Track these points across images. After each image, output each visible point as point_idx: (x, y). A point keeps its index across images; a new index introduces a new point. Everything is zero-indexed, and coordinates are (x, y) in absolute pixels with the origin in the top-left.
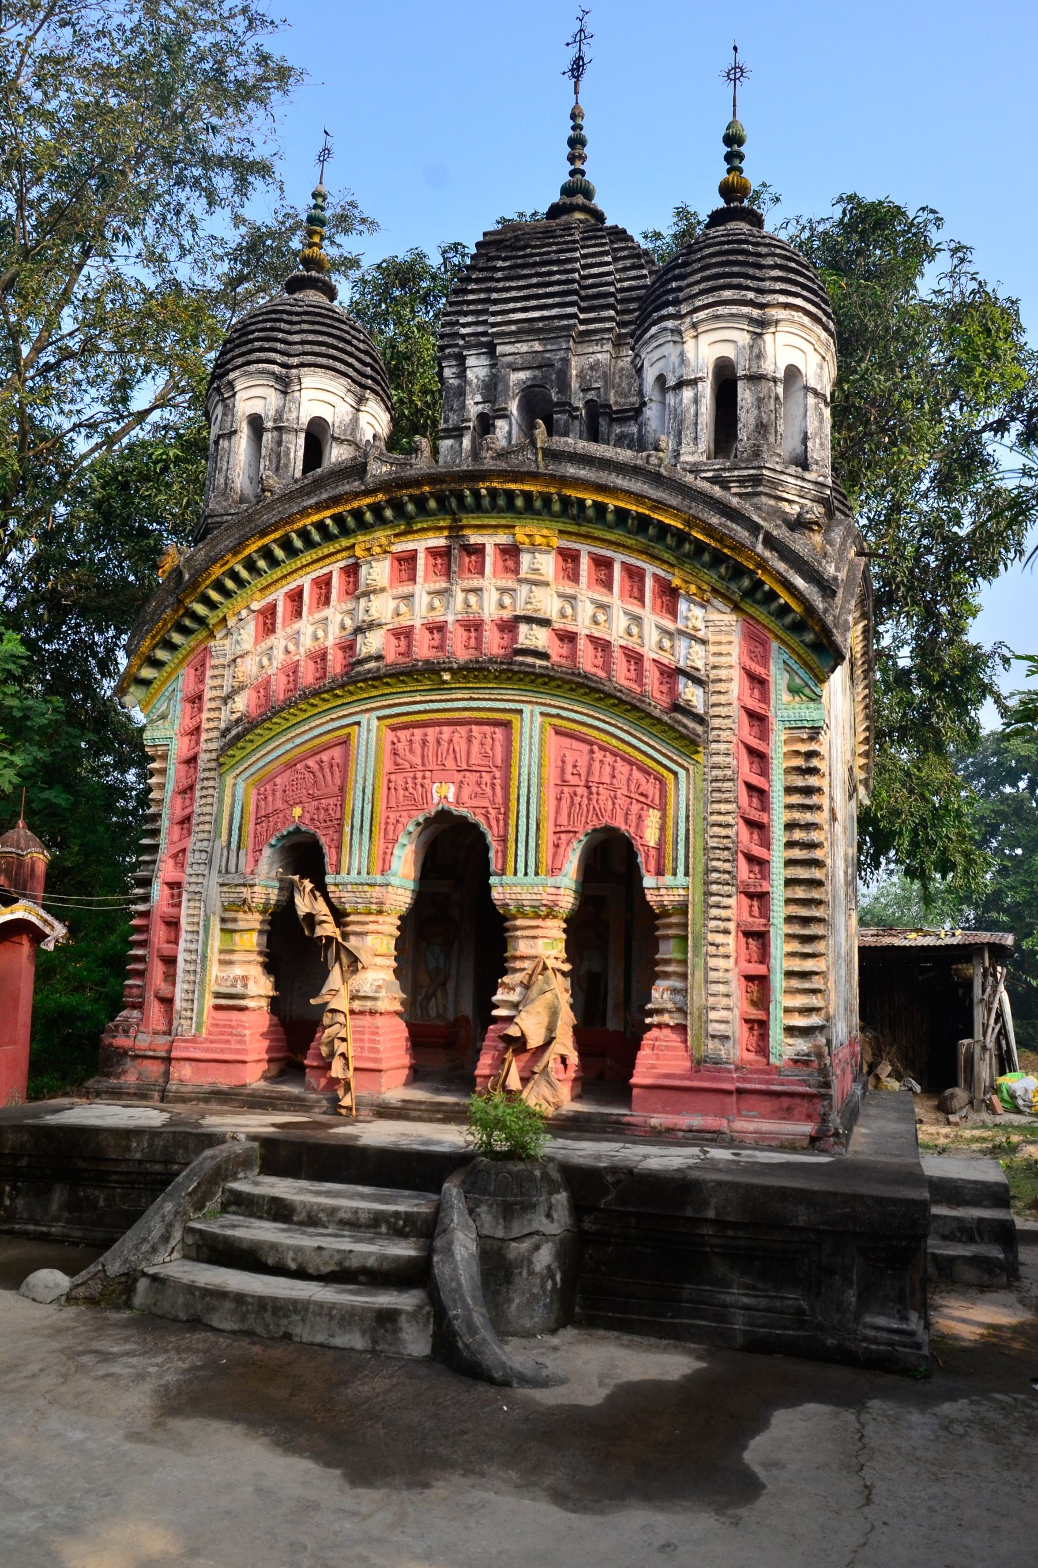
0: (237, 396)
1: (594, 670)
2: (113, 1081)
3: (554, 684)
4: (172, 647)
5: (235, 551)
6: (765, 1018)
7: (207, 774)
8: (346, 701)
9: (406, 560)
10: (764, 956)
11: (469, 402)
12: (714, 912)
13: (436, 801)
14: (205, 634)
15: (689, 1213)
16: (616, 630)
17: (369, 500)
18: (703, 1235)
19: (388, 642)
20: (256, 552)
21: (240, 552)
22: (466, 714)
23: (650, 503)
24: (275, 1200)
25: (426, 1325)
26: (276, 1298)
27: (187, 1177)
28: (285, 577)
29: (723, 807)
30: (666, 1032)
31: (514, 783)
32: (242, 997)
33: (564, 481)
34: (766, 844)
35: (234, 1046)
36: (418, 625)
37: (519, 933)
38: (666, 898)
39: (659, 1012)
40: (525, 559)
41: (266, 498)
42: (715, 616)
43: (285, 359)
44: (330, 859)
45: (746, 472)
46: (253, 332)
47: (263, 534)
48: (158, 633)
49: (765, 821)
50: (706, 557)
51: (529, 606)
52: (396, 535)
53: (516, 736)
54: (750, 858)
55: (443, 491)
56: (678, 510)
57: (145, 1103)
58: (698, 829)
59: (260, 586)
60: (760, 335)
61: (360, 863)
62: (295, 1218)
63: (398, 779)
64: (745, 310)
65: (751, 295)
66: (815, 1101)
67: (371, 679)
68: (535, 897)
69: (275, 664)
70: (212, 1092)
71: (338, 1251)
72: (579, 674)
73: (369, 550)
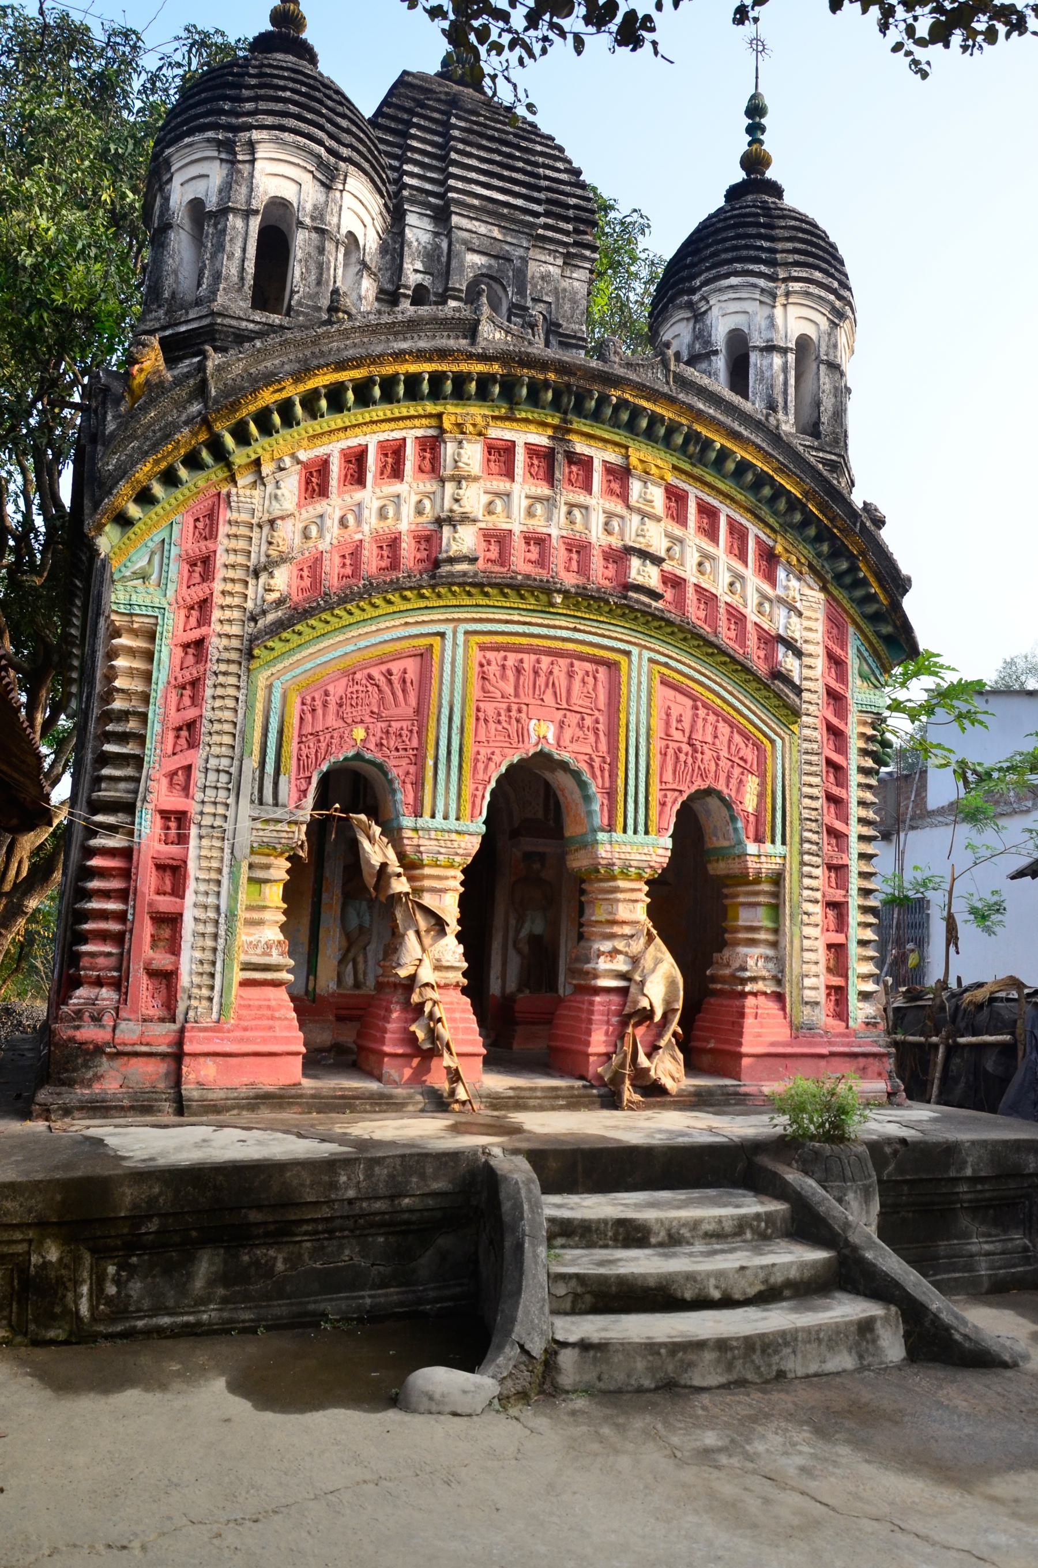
0: (258, 165)
1: (699, 623)
2: (82, 1092)
3: (669, 630)
4: (170, 479)
5: (298, 377)
6: (843, 984)
7: (223, 667)
9: (498, 450)
10: (841, 925)
11: (408, 266)
12: (807, 882)
13: (534, 739)
15: (952, 1174)
17: (480, 368)
18: (958, 1193)
20: (325, 386)
22: (570, 646)
23: (776, 465)
25: (897, 1327)
26: (763, 1334)
28: (346, 428)
30: (762, 999)
31: (622, 731)
33: (699, 415)
35: (278, 1033)
36: (517, 533)
37: (620, 896)
39: (754, 979)
40: (636, 486)
41: (340, 321)
42: (807, 591)
43: (333, 144)
44: (404, 796)
46: (284, 89)
47: (341, 366)
48: (164, 458)
49: (844, 796)
50: (812, 532)
51: (641, 539)
52: (494, 417)
53: (624, 679)
54: (832, 832)
55: (568, 386)
57: (149, 1119)
58: (795, 798)
59: (311, 433)
61: (447, 805)
62: (653, 1240)
64: (832, 297)
67: (471, 584)
68: (644, 858)
70: (257, 1097)
71: (762, 1267)
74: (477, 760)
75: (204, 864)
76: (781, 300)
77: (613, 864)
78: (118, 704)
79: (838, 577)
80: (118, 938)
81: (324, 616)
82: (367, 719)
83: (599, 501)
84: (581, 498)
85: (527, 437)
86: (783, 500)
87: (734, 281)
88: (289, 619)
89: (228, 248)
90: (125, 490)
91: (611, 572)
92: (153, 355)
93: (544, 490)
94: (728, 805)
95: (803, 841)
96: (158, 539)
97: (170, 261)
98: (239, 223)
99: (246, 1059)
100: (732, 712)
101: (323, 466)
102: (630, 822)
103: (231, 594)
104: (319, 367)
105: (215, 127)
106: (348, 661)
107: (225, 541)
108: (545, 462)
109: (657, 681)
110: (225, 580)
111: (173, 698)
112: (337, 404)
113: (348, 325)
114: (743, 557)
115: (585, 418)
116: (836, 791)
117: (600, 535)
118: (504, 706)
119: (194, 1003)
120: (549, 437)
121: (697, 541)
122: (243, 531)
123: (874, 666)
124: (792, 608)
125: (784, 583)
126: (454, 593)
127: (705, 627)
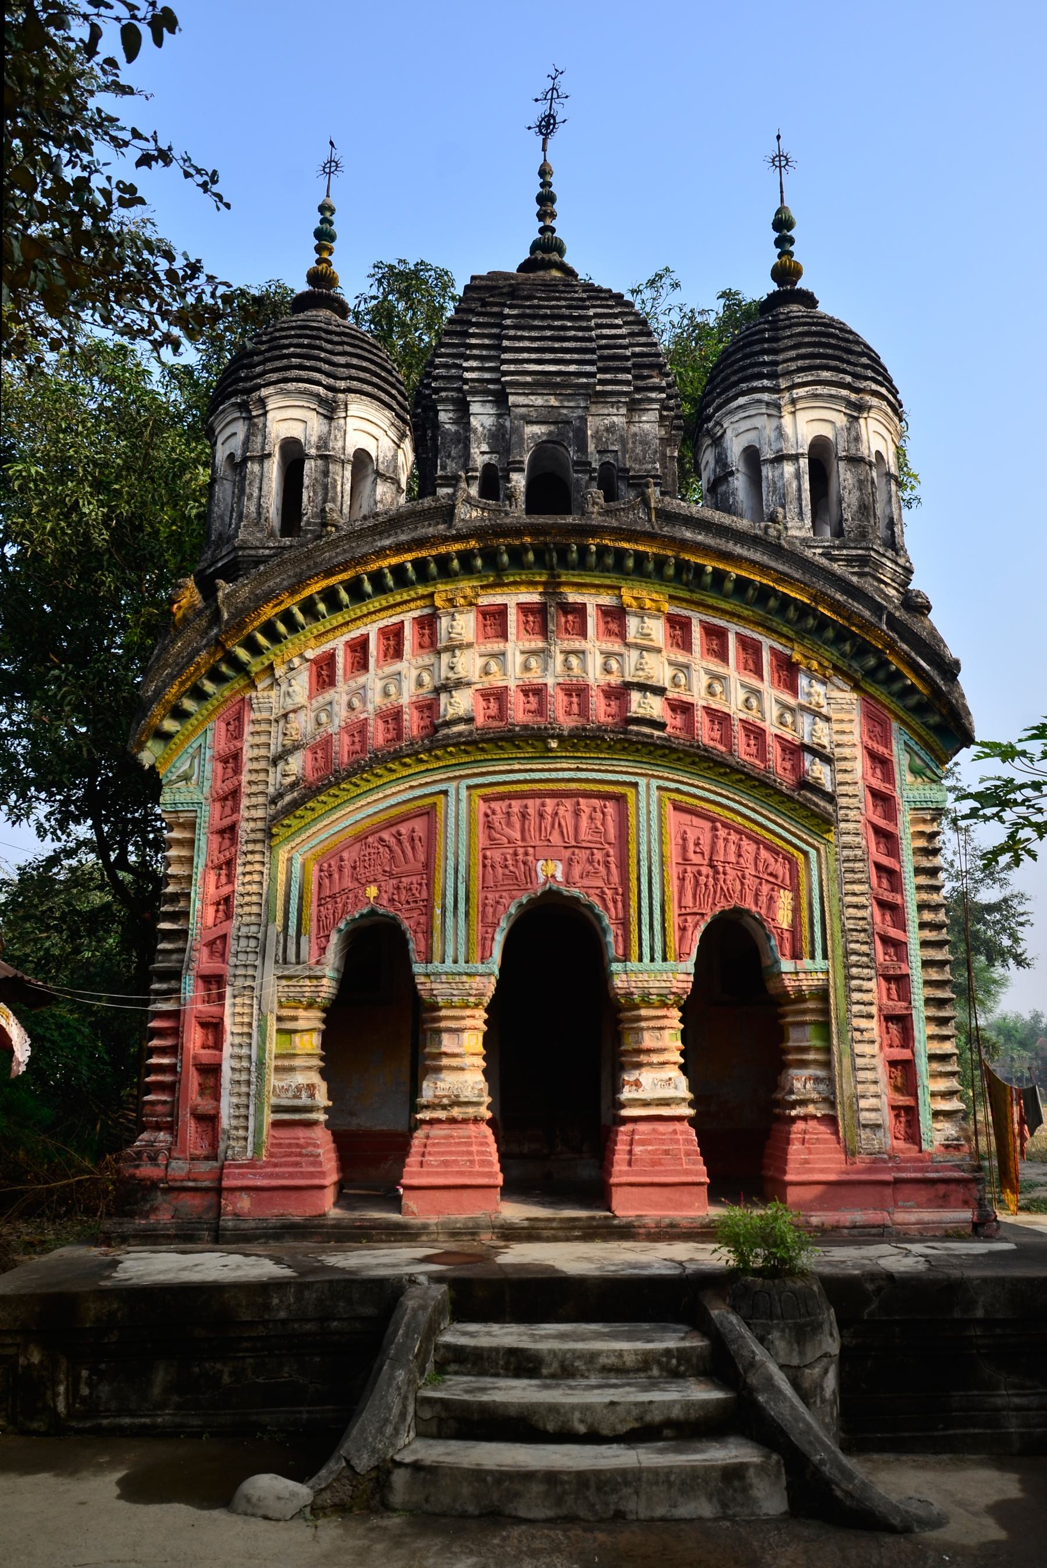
1: (712, 743)
3: (674, 756)
5: (293, 591)
8: (430, 767)
14: (243, 683)
16: (734, 703)
19: (477, 703)
22: (574, 786)
23: (775, 575)
31: (633, 862)
33: (684, 545)
47: (329, 573)
48: (188, 679)
50: (830, 633)
51: (641, 673)
53: (632, 810)
55: (546, 544)
56: (805, 584)
63: (495, 855)
69: (336, 722)
72: (698, 747)
78: (170, 889)
83: (595, 643)
84: (577, 644)
86: (792, 608)
91: (614, 708)
94: (760, 922)
100: (756, 828)
103: (255, 783)
104: (310, 578)
109: (669, 807)
114: (758, 672)
118: (511, 851)
123: (927, 759)
124: (817, 714)
125: (806, 690)
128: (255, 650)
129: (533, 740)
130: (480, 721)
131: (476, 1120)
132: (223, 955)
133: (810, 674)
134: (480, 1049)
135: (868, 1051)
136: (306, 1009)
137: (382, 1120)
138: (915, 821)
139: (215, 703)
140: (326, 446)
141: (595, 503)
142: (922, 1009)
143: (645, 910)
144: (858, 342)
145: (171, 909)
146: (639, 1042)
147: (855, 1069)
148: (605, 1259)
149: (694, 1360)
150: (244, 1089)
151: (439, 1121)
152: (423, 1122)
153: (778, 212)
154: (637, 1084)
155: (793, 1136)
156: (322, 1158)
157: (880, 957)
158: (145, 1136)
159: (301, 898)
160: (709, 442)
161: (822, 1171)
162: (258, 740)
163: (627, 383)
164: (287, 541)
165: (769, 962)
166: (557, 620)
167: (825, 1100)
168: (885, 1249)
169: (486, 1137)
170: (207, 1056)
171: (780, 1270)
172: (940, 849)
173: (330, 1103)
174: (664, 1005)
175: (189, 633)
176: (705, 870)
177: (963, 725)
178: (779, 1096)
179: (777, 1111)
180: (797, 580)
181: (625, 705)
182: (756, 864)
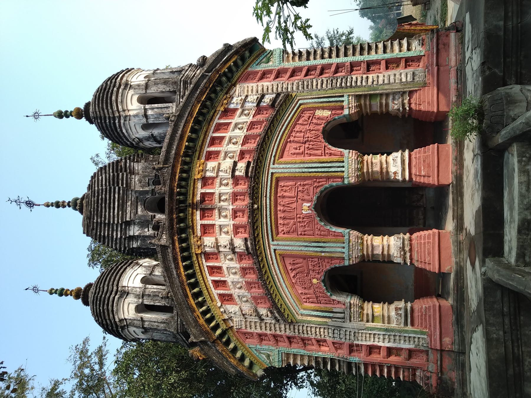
0: (126, 317)
1: (256, 143)
2: (456, 386)
3: (261, 158)
5: (193, 311)
7: (296, 331)
9: (205, 230)
10: (377, 62)
11: (147, 234)
12: (359, 83)
13: (310, 212)
14: (230, 332)
16: (240, 134)
17: (177, 244)
18: (513, 27)
21: (194, 309)
23: (190, 118)
24: (519, 232)
27: (512, 280)
28: (207, 289)
29: (315, 84)
30: (412, 101)
31: (303, 175)
32: (406, 310)
33: (177, 154)
34: (330, 66)
36: (233, 222)
37: (370, 170)
38: (353, 104)
40: (208, 174)
41: (171, 296)
43: (113, 293)
45: (182, 86)
46: (100, 310)
47: (186, 296)
49: (320, 66)
50: (213, 96)
51: (228, 171)
52: (194, 234)
53: (282, 175)
54: (336, 72)
55: (176, 209)
56: (193, 105)
58: (323, 93)
59: (211, 302)
60: (131, 86)
63: (300, 230)
64: (120, 90)
65: (115, 89)
66: (440, 34)
67: (255, 242)
68: (354, 162)
69: (246, 294)
70: (457, 324)
72: (257, 148)
73: (199, 247)
74: (320, 235)
75: (368, 339)
76: (127, 113)
77: (357, 175)
79: (229, 79)
80: (397, 369)
81: (274, 297)
82: (309, 278)
83: (216, 189)
84: (217, 196)
85: (198, 221)
86: (203, 111)
87: (124, 131)
88: (277, 309)
89: (155, 327)
90: (240, 368)
92: (195, 353)
93: (216, 212)
94: (328, 123)
95: (341, 87)
96: (255, 352)
97: (163, 339)
98: (146, 323)
99: (442, 326)
100: (290, 125)
101: (221, 296)
102: (339, 169)
103: (270, 328)
104: (188, 304)
105: (118, 331)
106: (289, 286)
107: (253, 329)
108: (206, 212)
109: (281, 160)
110: (266, 330)
111: (309, 347)
112: (200, 294)
113: (172, 294)
114: (228, 124)
115: (187, 198)
116: (318, 71)
117: (229, 188)
118: (298, 224)
119: (420, 344)
120: (197, 211)
121: (225, 146)
122: (248, 324)
123: (263, 56)
124: (245, 101)
126: (259, 248)
127: (257, 140)
128: (217, 326)
129: (254, 215)
130: (246, 235)
131: (410, 240)
132: (341, 344)
133: (229, 103)
134: (380, 238)
135: (381, 78)
136: (363, 310)
137: (410, 281)
138: (288, 61)
139: (238, 343)
140: (139, 295)
141: (161, 189)
142: (364, 56)
143: (323, 170)
144: (102, 85)
145: (322, 364)
146: (377, 172)
147: (389, 83)
148: (472, 188)
149: (523, 150)
150: (397, 338)
151: (411, 256)
152: (411, 263)
153: (56, 117)
154: (395, 173)
155: (417, 109)
156: (427, 306)
157: (343, 74)
158: (418, 381)
159: (317, 311)
160: (141, 144)
161: (433, 96)
162: (253, 326)
163: (123, 175)
164: (175, 312)
165: (345, 119)
166: (207, 204)
167: (402, 96)
168: (468, 68)
169: (418, 236)
170: (383, 353)
171: (480, 113)
172: (299, 51)
173: (403, 300)
174: (362, 162)
175: (210, 353)
176: (307, 146)
177: (249, 42)
178: (400, 115)
179: (407, 116)
180: (191, 108)
181: (240, 177)
182: (305, 125)
